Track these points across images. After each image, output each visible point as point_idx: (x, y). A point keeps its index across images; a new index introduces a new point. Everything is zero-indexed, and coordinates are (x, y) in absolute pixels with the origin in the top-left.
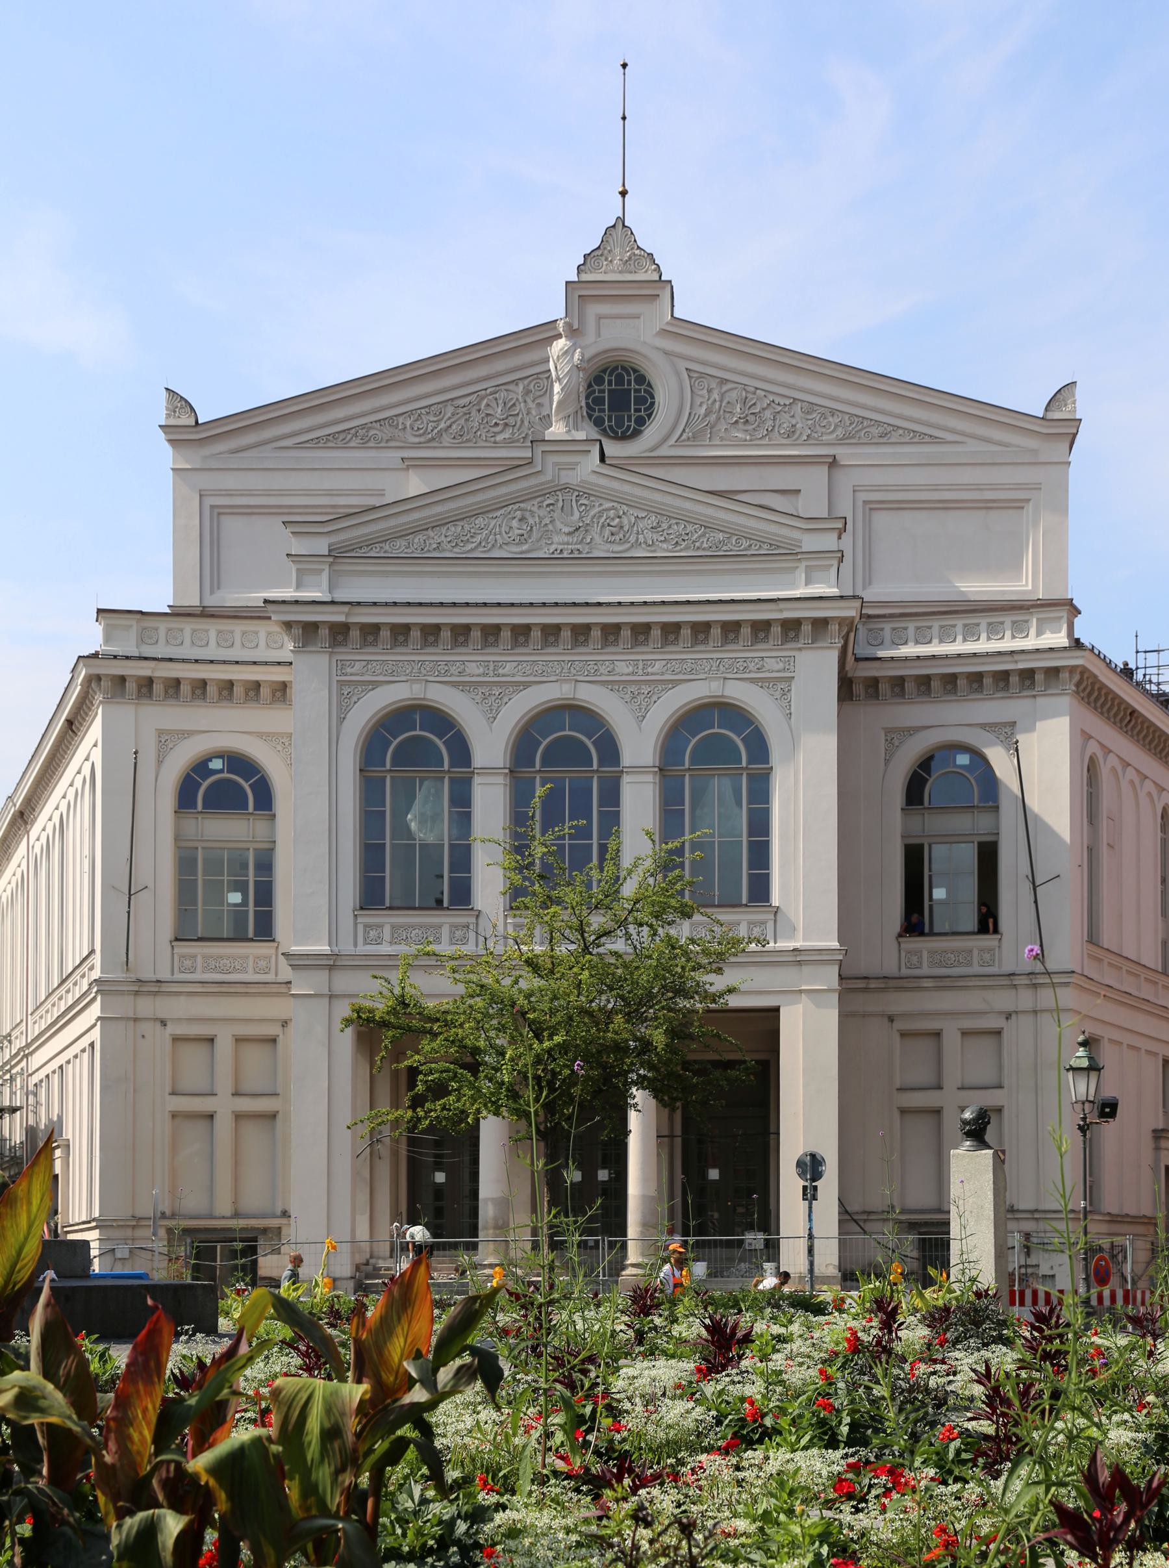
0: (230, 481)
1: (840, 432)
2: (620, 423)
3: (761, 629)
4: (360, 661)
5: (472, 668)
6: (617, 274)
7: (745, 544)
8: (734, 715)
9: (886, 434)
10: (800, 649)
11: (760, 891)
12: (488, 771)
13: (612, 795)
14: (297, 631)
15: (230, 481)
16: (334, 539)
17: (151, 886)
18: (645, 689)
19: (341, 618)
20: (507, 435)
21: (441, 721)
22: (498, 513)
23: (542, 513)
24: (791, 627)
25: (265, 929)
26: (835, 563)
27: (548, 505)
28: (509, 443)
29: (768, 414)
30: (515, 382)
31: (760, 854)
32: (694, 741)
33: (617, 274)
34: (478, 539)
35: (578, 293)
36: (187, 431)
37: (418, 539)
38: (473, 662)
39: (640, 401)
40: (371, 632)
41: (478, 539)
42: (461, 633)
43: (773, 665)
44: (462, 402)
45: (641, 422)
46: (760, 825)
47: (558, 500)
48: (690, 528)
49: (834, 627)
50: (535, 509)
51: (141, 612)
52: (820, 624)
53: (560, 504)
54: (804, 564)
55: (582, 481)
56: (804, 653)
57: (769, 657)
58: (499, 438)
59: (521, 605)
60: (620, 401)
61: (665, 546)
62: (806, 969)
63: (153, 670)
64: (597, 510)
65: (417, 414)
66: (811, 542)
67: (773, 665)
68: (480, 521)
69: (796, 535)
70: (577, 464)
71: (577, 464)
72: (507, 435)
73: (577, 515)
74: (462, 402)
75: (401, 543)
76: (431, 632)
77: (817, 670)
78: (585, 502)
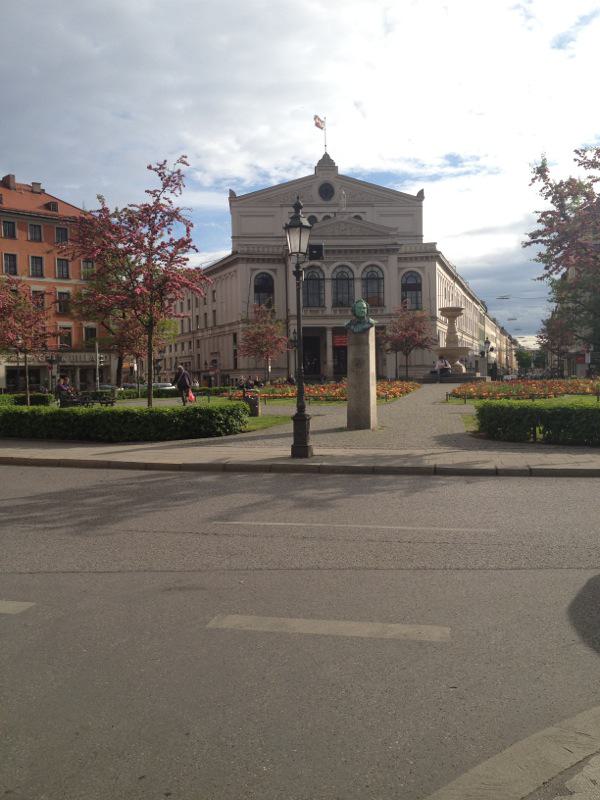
6: (326, 163)
33: (326, 163)
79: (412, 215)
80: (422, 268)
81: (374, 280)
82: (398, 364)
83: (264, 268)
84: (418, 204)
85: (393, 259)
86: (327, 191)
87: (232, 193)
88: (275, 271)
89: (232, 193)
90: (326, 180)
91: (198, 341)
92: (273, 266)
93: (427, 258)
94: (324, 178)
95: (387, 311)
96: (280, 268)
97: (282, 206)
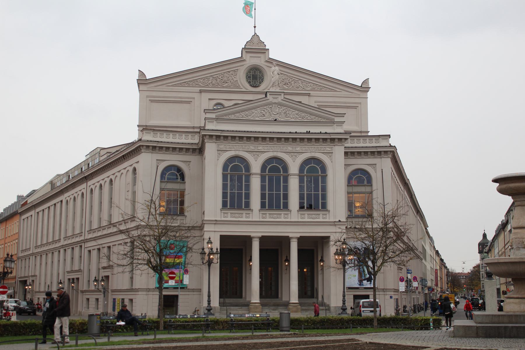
0: (154, 94)
1: (310, 88)
2: (255, 83)
4: (223, 145)
5: (252, 147)
7: (320, 119)
8: (318, 161)
9: (321, 88)
11: (324, 206)
12: (256, 174)
13: (286, 180)
15: (154, 94)
16: (217, 114)
18: (295, 154)
19: (219, 134)
20: (226, 85)
21: (243, 160)
24: (332, 140)
25: (182, 212)
28: (226, 87)
29: (293, 82)
30: (229, 72)
31: (324, 197)
32: (307, 167)
35: (246, 50)
36: (143, 81)
37: (237, 115)
38: (252, 146)
39: (249, 77)
40: (226, 137)
42: (249, 138)
44: (215, 76)
45: (260, 83)
46: (324, 189)
52: (340, 140)
57: (327, 148)
58: (225, 85)
59: (265, 132)
60: (255, 77)
65: (204, 79)
66: (337, 119)
67: (328, 149)
69: (333, 117)
72: (226, 85)
73: (277, 110)
74: (215, 76)
75: (233, 115)
77: (339, 151)
79: (355, 107)
80: (373, 165)
82: (347, 285)
83: (174, 159)
84: (362, 95)
85: (339, 151)
86: (255, 76)
87: (141, 73)
88: (187, 162)
89: (141, 73)
90: (254, 68)
91: (90, 251)
92: (187, 158)
93: (379, 153)
94: (251, 61)
95: (331, 218)
96: (194, 159)
97: (201, 92)
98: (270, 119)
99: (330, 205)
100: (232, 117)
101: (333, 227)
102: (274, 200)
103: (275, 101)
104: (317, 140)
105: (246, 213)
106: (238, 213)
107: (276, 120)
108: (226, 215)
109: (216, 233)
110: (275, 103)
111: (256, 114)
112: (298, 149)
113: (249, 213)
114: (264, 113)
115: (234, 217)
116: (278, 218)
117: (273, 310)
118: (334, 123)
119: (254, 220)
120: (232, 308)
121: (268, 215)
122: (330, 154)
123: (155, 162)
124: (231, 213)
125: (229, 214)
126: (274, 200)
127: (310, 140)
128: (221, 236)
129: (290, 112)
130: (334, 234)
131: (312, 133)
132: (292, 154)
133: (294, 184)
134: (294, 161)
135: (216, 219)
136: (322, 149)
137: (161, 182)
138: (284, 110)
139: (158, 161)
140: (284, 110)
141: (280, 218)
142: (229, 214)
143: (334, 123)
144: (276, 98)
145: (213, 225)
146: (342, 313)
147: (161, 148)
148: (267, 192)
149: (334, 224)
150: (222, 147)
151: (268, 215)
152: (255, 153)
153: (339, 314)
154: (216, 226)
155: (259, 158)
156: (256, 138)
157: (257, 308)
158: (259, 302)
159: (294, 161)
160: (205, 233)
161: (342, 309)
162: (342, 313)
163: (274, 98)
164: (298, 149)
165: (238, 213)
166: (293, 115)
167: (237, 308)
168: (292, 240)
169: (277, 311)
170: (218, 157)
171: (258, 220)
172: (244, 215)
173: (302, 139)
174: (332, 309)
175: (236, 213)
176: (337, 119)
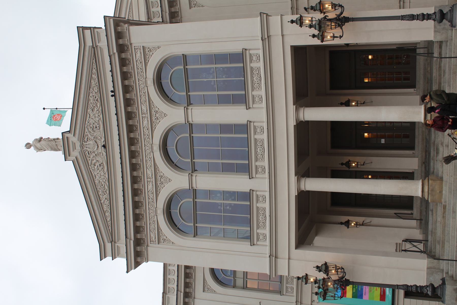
3: (123, 62)
4: (150, 234)
10: (131, 44)
11: (239, 57)
14: (139, 259)
17: (260, 300)
18: (153, 113)
19: (132, 242)
22: (94, 174)
23: (92, 156)
24: (122, 49)
26: (96, 30)
27: (89, 154)
34: (103, 183)
38: (148, 187)
40: (137, 230)
41: (103, 183)
42: (135, 193)
43: (139, 55)
47: (87, 150)
48: (91, 95)
49: (119, 29)
50: (91, 159)
51: (163, 293)
53: (87, 149)
54: (98, 44)
55: (78, 140)
56: (132, 42)
57: (136, 57)
61: (98, 106)
62: (271, 33)
63: (181, 292)
64: (88, 133)
66: (89, 43)
67: (139, 55)
68: (97, 182)
70: (72, 142)
71: (72, 142)
73: (91, 142)
76: (136, 205)
78: (86, 138)
81: (177, 79)
85: (138, 36)
98: (105, 154)
99: (236, 48)
100: (108, 214)
101: (273, 39)
102: (235, 149)
103: (78, 145)
104: (125, 76)
105: (257, 202)
106: (258, 216)
107: (104, 146)
108: (261, 237)
109: (292, 256)
110: (82, 146)
111: (100, 176)
112: (144, 108)
113: (257, 196)
114: (97, 164)
115: (264, 223)
116: (262, 145)
117: (438, 153)
118: (94, 48)
119: (267, 189)
120: (430, 227)
121: (257, 164)
122: (147, 50)
123: (207, 295)
124: (258, 228)
125: (259, 231)
126: (235, 149)
127: (127, 89)
128: (297, 247)
129: (92, 121)
130: (286, 38)
131: (113, 87)
132: (154, 118)
133: (202, 115)
134: (165, 115)
135: (268, 255)
136: (140, 66)
137: (234, 287)
138: (90, 132)
139: (206, 289)
140: (90, 132)
141: (262, 141)
142: (259, 231)
143: (94, 48)
144: (74, 144)
145: (279, 260)
146: (451, 21)
147: (187, 285)
148: (221, 161)
149: (266, 39)
150: (153, 235)
151: (257, 164)
152: (158, 183)
153: (452, 26)
154: (280, 254)
155: (166, 175)
156: (135, 180)
157: (432, 190)
158: (420, 182)
159: (165, 115)
160: (292, 274)
161: (441, 21)
162: (451, 21)
163: (74, 148)
164: (144, 108)
165: (258, 216)
166: (94, 117)
167: (430, 218)
168: (301, 118)
169: (441, 149)
170: (169, 241)
171: (267, 181)
172: (259, 205)
173: (128, 103)
174: (439, 38)
175: (258, 220)
176: (89, 43)
